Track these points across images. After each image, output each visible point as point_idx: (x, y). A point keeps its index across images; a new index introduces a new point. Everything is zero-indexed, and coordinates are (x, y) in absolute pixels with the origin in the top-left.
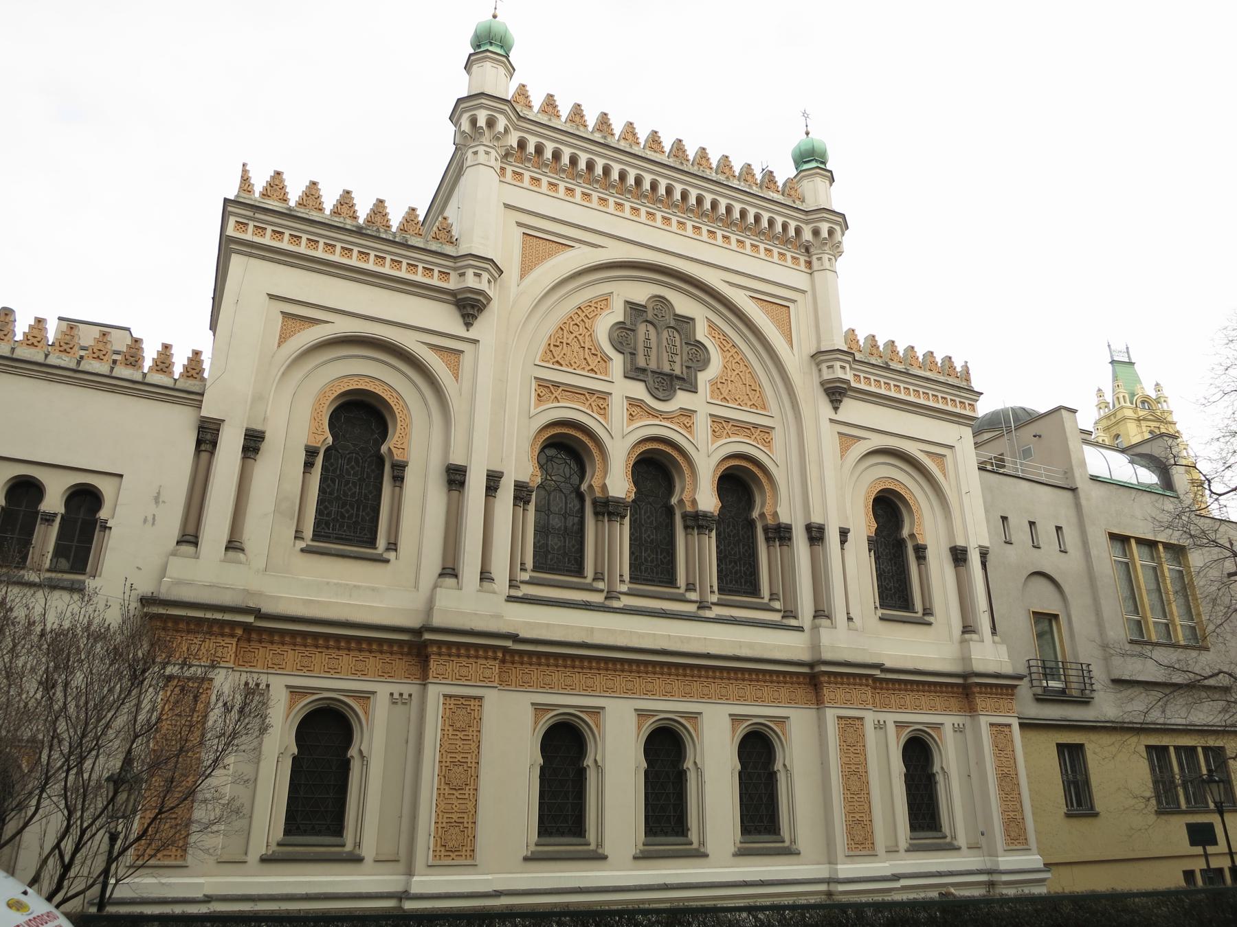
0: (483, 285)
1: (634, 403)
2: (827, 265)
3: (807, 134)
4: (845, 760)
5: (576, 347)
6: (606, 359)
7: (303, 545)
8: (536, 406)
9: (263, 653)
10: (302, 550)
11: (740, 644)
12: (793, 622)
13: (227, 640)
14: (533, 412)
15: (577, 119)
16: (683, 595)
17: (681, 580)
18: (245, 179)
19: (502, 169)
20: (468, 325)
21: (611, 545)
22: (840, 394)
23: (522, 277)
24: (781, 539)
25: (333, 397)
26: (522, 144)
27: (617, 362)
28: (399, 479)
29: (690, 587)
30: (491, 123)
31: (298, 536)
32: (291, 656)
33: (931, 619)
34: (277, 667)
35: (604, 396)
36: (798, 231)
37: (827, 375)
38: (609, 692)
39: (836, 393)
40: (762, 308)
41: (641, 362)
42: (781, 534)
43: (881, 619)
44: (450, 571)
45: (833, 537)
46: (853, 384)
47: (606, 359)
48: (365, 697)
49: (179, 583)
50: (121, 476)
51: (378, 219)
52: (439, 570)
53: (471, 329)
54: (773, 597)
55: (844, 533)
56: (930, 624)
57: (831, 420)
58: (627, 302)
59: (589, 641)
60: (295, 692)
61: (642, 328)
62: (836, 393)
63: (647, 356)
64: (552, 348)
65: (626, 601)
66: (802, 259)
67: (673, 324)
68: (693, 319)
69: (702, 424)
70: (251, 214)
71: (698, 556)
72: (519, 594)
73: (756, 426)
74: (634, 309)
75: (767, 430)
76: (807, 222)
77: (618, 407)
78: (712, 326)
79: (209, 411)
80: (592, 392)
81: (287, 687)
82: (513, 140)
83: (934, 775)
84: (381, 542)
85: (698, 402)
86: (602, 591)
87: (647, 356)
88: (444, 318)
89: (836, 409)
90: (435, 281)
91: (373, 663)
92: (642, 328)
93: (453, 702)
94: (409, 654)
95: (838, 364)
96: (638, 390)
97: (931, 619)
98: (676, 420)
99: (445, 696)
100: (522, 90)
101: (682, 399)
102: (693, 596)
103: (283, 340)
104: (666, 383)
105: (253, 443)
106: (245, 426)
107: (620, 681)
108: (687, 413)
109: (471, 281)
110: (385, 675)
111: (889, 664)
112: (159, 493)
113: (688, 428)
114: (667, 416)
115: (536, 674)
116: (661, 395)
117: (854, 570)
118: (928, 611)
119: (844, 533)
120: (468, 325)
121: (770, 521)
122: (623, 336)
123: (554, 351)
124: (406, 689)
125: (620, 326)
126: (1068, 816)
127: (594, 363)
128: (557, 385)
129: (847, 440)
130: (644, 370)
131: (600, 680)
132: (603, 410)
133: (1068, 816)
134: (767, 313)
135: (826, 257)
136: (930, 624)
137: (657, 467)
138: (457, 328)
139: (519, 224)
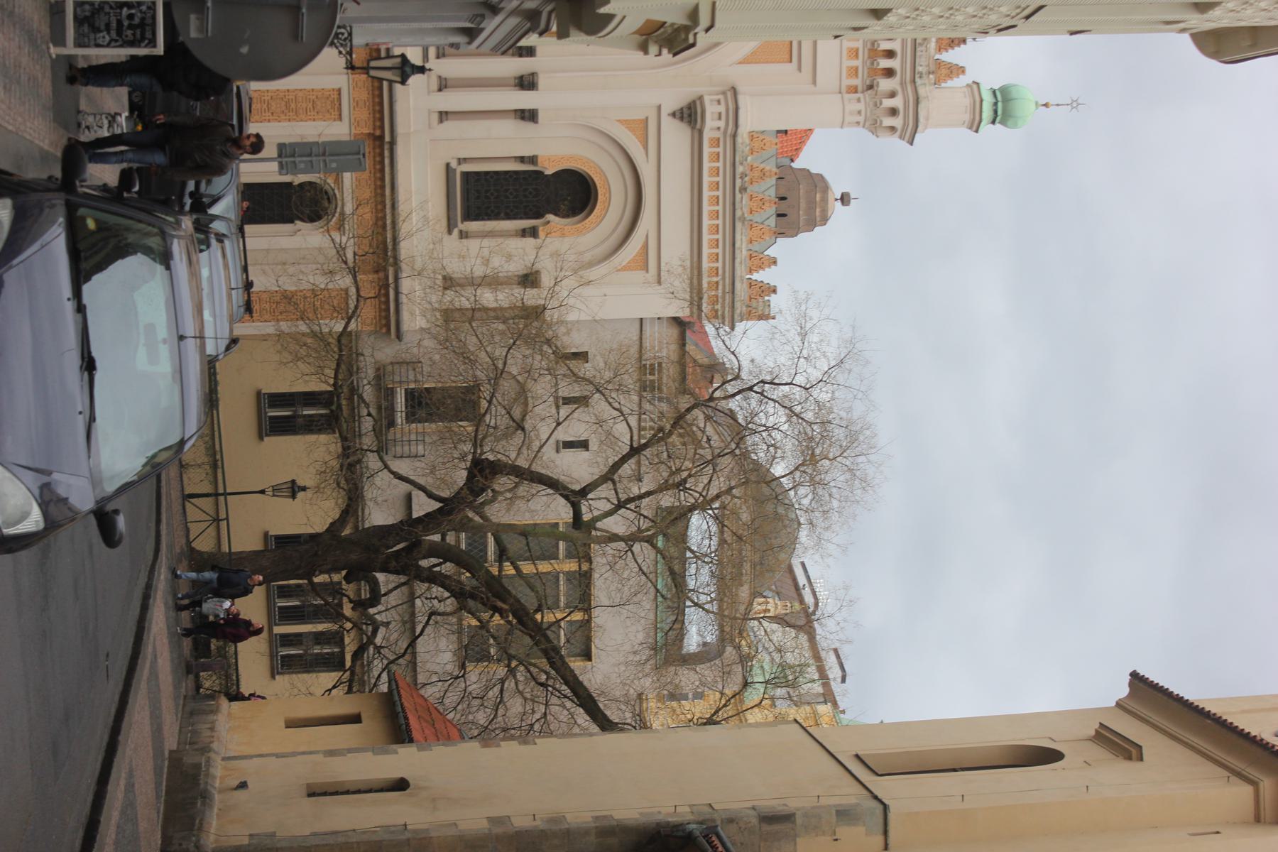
3: (1046, 105)
4: (300, 94)
22: (690, 116)
37: (707, 99)
39: (690, 114)
43: (448, 165)
45: (524, 100)
46: (708, 135)
55: (529, 116)
56: (450, 232)
57: (659, 107)
62: (690, 114)
66: (857, 82)
76: (903, 84)
83: (292, 222)
89: (674, 115)
95: (722, 108)
117: (499, 145)
118: (463, 235)
119: (529, 116)
126: (259, 393)
129: (640, 128)
133: (259, 393)
135: (861, 106)
136: (450, 232)
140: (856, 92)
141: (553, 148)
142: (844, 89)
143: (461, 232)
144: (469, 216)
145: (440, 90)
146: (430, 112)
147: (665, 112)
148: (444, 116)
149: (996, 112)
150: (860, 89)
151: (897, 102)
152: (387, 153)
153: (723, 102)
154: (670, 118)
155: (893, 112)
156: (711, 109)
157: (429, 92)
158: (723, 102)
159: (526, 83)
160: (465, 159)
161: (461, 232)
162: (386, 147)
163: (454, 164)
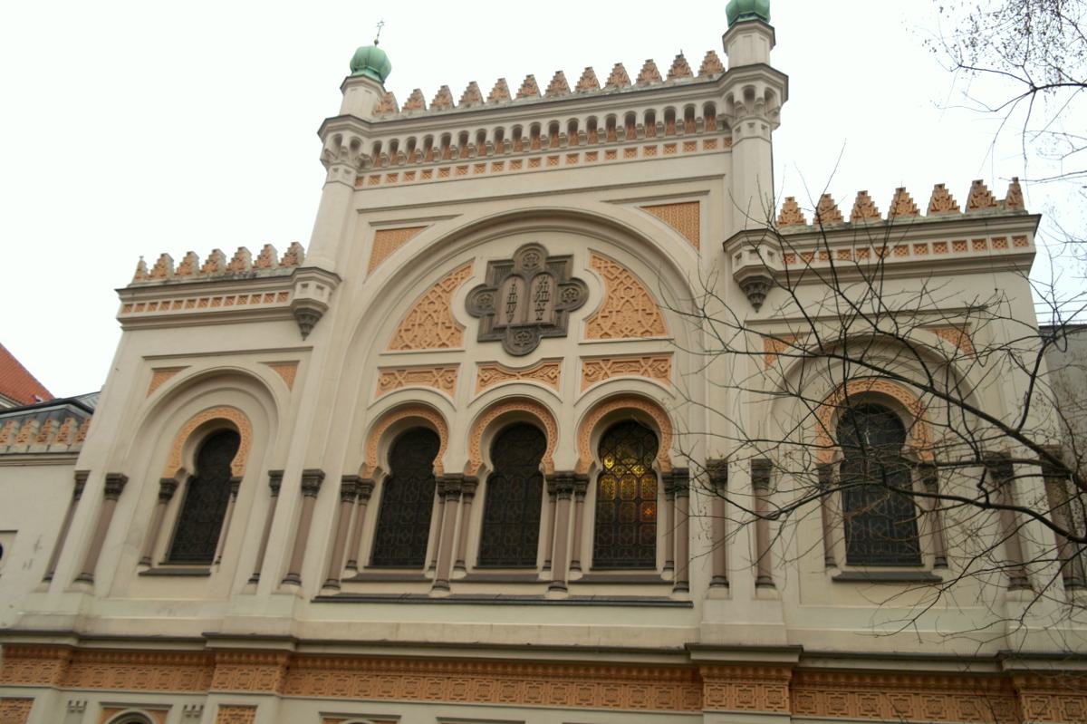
0: (311, 293)
1: (488, 367)
2: (745, 131)
5: (429, 325)
6: (460, 329)
7: (145, 569)
8: (378, 394)
9: (89, 673)
10: (142, 574)
11: (589, 631)
12: (680, 596)
13: (53, 662)
14: (372, 401)
15: (440, 101)
16: (537, 576)
17: (540, 561)
18: (139, 270)
19: (359, 180)
20: (305, 335)
21: (458, 529)
22: (756, 286)
23: (369, 272)
24: (679, 489)
25: (191, 431)
26: (377, 148)
27: (472, 327)
28: (236, 494)
29: (547, 568)
30: (338, 140)
31: (146, 560)
32: (110, 674)
33: (941, 573)
34: (97, 686)
35: (452, 368)
36: (710, 110)
37: (735, 269)
38: (410, 697)
39: (754, 286)
40: (659, 216)
41: (502, 320)
42: (678, 483)
43: (836, 580)
44: (255, 580)
46: (777, 265)
47: (460, 329)
48: (163, 710)
49: (28, 615)
50: (15, 532)
51: (237, 265)
52: (251, 576)
53: (308, 338)
54: (670, 565)
58: (491, 262)
59: (391, 638)
60: (108, 707)
61: (507, 287)
62: (754, 286)
63: (510, 313)
64: (403, 333)
65: (457, 590)
66: (720, 140)
67: (542, 266)
68: (570, 256)
69: (572, 372)
70: (130, 296)
71: (568, 530)
72: (331, 592)
73: (646, 357)
74: (501, 269)
75: (663, 357)
76: (719, 94)
77: (467, 377)
78: (596, 256)
79: (81, 465)
80: (439, 367)
81: (102, 703)
82: (366, 148)
84: (216, 558)
85: (569, 348)
86: (430, 581)
87: (510, 313)
88: (281, 335)
90: (275, 304)
91: (176, 675)
92: (507, 287)
93: (228, 712)
94: (207, 665)
96: (495, 352)
97: (941, 573)
98: (537, 374)
99: (223, 707)
100: (388, 99)
101: (548, 348)
102: (545, 576)
103: (151, 391)
104: (524, 336)
105: (115, 486)
106: (107, 471)
107: (424, 684)
108: (554, 363)
109: (298, 294)
110: (187, 686)
111: (810, 646)
112: (38, 541)
113: (553, 380)
114: (529, 372)
115: (330, 679)
116: (520, 350)
118: (942, 562)
120: (305, 335)
121: (665, 469)
122: (481, 302)
123: (403, 339)
124: (197, 701)
125: (480, 289)
127: (444, 336)
128: (401, 369)
130: (503, 329)
131: (401, 684)
132: (450, 385)
134: (666, 219)
135: (744, 125)
137: (518, 434)
138: (294, 340)
139: (372, 224)
140: (730, 139)
141: (801, 434)
142: (729, 149)
143: (936, 566)
144: (917, 561)
145: (727, 585)
146: (757, 597)
147: (753, 316)
148: (763, 581)
149: (750, 15)
150: (727, 136)
151: (738, 93)
152: (820, 664)
153: (738, 252)
154: (762, 310)
155: (749, 94)
156: (748, 260)
157: (729, 598)
158: (738, 252)
159: (718, 475)
160: (826, 559)
161: (936, 566)
162: (809, 664)
163: (835, 572)
